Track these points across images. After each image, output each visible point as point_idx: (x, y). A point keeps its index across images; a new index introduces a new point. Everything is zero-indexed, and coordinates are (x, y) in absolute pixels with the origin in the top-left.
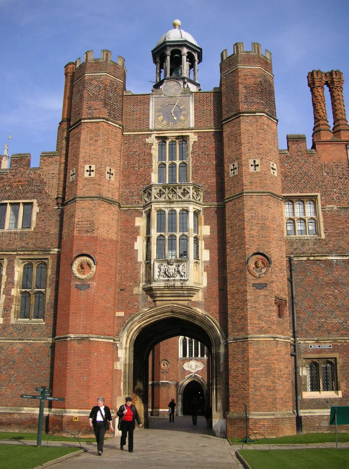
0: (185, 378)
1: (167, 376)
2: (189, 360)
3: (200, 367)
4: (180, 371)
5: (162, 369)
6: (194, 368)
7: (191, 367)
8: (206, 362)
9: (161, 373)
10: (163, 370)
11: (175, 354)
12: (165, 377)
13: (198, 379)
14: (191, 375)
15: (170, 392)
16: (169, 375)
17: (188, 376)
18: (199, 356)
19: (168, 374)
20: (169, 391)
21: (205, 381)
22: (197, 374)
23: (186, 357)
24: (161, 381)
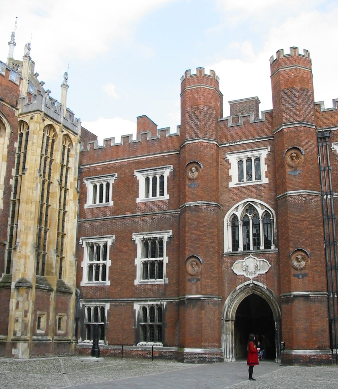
0: (235, 291)
1: (197, 287)
2: (243, 256)
3: (263, 268)
4: (226, 277)
5: (188, 273)
6: (253, 270)
7: (246, 270)
8: (273, 257)
9: (187, 280)
10: (191, 275)
11: (214, 245)
12: (194, 288)
13: (262, 291)
14: (246, 283)
15: (203, 316)
16: (201, 284)
17: (241, 286)
18: (262, 248)
19: (199, 283)
20: (202, 313)
21: (274, 294)
22: (258, 281)
23: (237, 250)
24: (187, 296)
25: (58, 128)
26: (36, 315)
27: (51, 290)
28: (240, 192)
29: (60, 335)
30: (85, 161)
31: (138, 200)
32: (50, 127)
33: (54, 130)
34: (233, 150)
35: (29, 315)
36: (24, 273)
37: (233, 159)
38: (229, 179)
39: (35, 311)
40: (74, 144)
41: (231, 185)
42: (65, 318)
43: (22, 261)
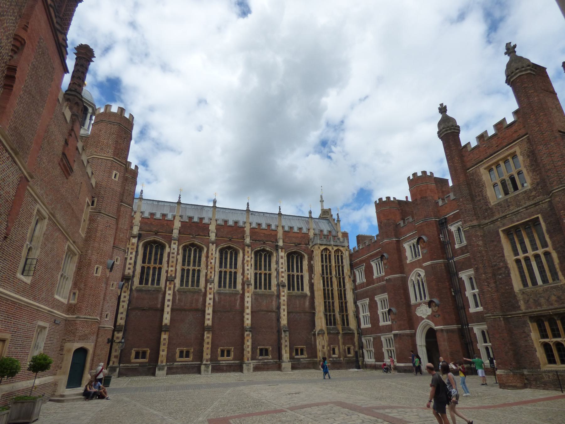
25: (330, 248)
26: (330, 348)
27: (338, 333)
28: (414, 265)
29: (349, 357)
30: (353, 259)
31: (374, 277)
32: (326, 249)
33: (329, 250)
34: (405, 240)
35: (325, 348)
36: (322, 326)
37: (406, 246)
38: (406, 258)
39: (329, 345)
40: (344, 252)
41: (408, 262)
42: (352, 348)
43: (320, 320)
